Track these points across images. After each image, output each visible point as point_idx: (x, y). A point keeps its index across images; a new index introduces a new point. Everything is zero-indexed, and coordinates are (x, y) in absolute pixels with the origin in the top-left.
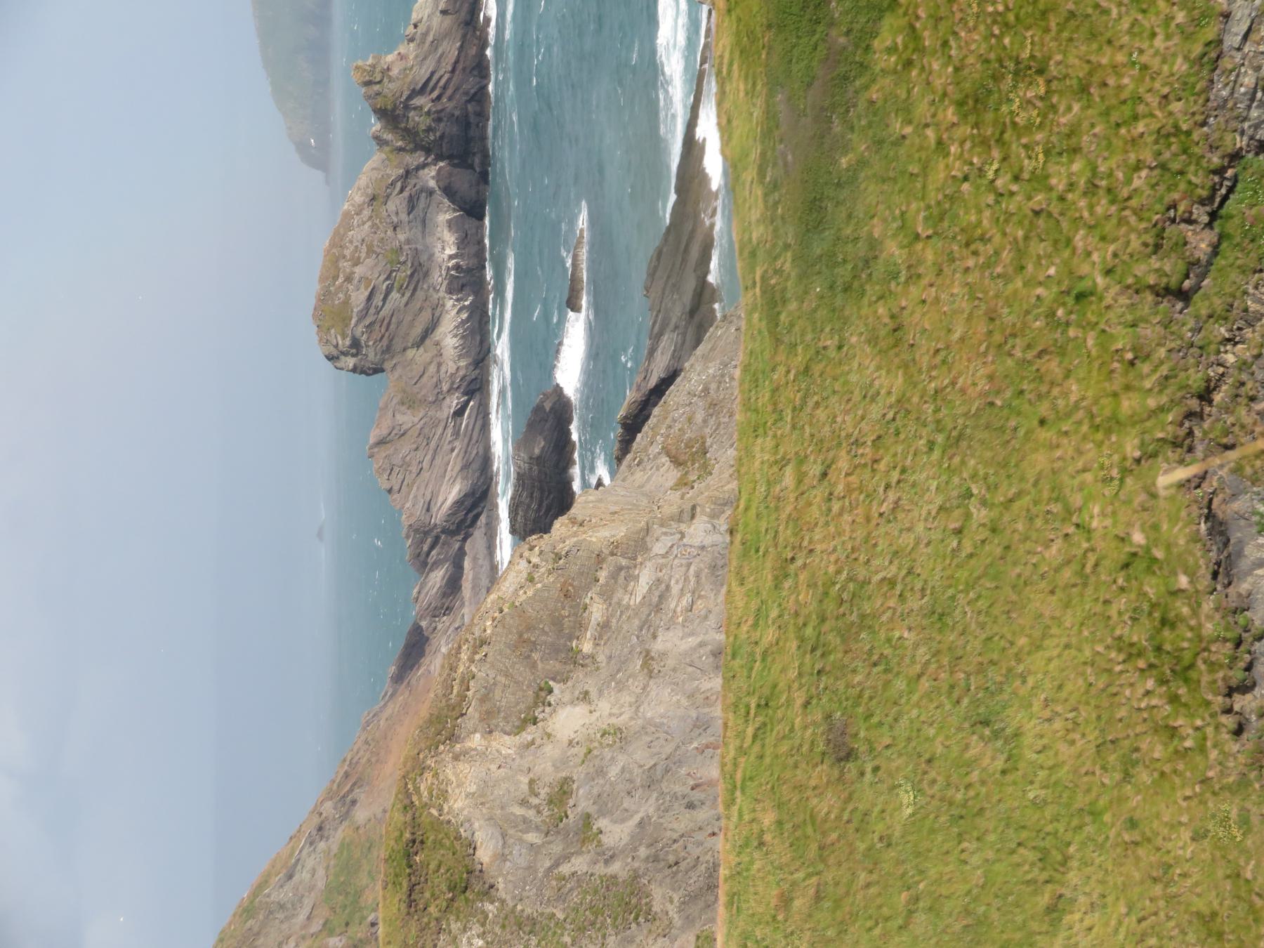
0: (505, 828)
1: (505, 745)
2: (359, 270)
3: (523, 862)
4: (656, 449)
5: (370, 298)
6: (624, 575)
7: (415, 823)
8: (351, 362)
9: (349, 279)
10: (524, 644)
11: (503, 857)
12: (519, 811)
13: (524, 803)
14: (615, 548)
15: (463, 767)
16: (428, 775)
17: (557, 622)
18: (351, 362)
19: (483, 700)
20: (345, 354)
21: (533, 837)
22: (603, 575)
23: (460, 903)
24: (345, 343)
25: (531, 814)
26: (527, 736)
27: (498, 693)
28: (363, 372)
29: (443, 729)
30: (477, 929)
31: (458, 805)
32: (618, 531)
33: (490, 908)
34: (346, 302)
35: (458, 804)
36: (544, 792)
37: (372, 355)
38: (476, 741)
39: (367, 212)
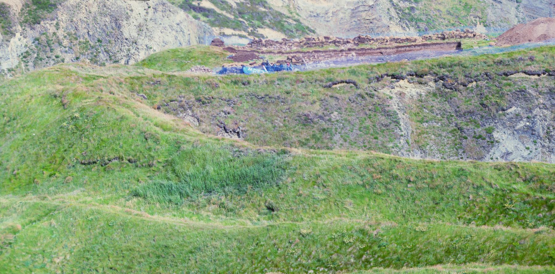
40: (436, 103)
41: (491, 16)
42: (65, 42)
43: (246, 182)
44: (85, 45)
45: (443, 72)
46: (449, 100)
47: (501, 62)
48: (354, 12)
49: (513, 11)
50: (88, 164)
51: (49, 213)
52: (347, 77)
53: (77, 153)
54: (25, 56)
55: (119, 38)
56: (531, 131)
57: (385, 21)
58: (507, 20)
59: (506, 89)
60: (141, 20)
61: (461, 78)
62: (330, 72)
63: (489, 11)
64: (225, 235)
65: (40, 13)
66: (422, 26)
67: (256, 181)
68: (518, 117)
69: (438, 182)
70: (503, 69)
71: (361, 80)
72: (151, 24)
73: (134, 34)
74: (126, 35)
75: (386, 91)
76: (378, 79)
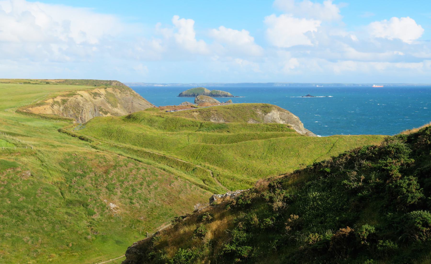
1: (278, 116)
6: (297, 128)
8: (196, 99)
10: (289, 118)
14: (299, 127)
17: (291, 121)
18: (196, 99)
24: (198, 99)
29: (279, 110)
32: (301, 127)
35: (273, 111)
37: (197, 102)
38: (278, 113)
40: (200, 115)
41: (119, 102)
43: (220, 128)
48: (101, 102)
50: (183, 126)
51: (189, 134)
54: (63, 110)
55: (79, 107)
56: (215, 119)
67: (223, 127)
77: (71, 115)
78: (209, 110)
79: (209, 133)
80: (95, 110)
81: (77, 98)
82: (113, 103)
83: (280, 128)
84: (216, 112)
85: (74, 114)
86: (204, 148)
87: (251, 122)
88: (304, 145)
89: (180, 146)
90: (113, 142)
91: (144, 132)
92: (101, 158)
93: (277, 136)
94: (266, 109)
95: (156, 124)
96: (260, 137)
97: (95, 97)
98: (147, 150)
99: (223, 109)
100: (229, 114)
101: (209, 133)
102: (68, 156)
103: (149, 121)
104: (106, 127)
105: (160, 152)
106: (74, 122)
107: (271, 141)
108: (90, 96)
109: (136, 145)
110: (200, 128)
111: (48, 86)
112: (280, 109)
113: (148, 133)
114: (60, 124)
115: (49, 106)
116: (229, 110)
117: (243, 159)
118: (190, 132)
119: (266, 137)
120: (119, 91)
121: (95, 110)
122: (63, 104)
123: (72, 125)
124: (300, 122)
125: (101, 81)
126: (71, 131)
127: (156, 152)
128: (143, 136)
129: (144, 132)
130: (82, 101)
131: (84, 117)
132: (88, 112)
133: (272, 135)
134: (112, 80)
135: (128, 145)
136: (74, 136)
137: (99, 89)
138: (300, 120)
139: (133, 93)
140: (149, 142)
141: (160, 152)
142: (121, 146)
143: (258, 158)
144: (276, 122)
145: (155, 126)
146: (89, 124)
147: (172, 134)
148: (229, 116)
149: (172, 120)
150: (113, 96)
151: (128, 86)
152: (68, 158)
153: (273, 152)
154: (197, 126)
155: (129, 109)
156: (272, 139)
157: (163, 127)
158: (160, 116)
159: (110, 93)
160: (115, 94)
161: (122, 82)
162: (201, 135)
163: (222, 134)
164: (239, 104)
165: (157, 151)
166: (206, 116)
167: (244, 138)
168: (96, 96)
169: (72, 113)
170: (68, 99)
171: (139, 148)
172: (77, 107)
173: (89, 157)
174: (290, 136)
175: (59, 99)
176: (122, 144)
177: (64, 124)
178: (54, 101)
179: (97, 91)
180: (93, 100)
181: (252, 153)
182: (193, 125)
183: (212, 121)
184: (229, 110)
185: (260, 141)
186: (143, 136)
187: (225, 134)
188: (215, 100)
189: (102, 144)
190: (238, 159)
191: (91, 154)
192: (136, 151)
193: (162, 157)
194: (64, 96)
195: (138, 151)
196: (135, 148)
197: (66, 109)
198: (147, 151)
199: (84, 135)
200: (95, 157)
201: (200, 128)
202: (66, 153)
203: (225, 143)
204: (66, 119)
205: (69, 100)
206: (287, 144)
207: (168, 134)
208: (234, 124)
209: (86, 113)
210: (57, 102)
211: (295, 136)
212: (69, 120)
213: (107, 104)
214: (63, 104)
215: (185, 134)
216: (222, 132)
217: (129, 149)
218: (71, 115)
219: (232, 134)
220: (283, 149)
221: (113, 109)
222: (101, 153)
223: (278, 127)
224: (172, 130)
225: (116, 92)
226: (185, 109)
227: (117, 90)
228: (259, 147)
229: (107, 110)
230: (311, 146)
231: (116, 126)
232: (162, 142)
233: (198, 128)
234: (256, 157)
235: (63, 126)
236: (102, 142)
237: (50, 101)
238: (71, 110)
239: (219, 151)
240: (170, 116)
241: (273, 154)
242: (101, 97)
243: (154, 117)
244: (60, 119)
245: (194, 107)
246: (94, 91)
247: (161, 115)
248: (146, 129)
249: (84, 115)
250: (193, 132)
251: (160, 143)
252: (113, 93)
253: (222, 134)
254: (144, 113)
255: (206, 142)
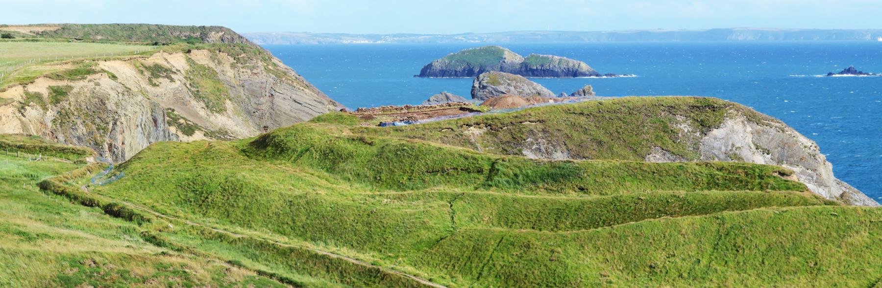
0: (726, 139)
1: (749, 139)
2: (512, 88)
3: (715, 145)
4: (844, 189)
5: (503, 93)
7: (720, 108)
8: (477, 85)
9: (509, 84)
10: (783, 145)
11: (715, 138)
12: (730, 143)
13: (733, 145)
14: (820, 175)
15: (741, 125)
16: (736, 112)
17: (792, 156)
18: (477, 85)
19: (763, 131)
20: (480, 83)
21: (723, 149)
22: (809, 171)
23: (697, 124)
24: (484, 83)
25: (730, 148)
26: (753, 146)
27: (766, 136)
28: (472, 90)
29: (751, 118)
30: (690, 130)
31: (729, 122)
32: (824, 176)
33: (698, 134)
34: (500, 84)
35: (729, 123)
36: (737, 152)
37: (480, 93)
38: (749, 129)
39: (534, 91)
40: (488, 137)
41: (232, 95)
42: (76, 113)
43: (557, 177)
44: (87, 115)
45: (489, 122)
46: (496, 136)
47: (516, 117)
49: (242, 92)
50: (434, 172)
51: (456, 197)
52: (448, 126)
53: (420, 166)
54: (54, 121)
55: (106, 110)
56: (540, 150)
57: (188, 98)
58: (240, 97)
59: (524, 130)
60: (116, 100)
61: (500, 125)
62: (438, 123)
63: (229, 91)
64: (591, 202)
65: (59, 97)
66: (206, 100)
67: (563, 176)
68: (532, 143)
69: (672, 172)
70: (519, 120)
71: (454, 127)
72: (123, 103)
73: (114, 108)
74: (109, 108)
75: (466, 132)
76: (462, 126)
77: (79, 138)
78: (517, 121)
79: (519, 195)
80: (155, 121)
81: (98, 84)
82: (212, 97)
83: (754, 177)
84: (540, 126)
85: (91, 133)
86: (503, 243)
87: (656, 158)
88: (834, 234)
89: (425, 235)
90: (213, 223)
91: (309, 189)
92: (175, 272)
93: (743, 204)
94: (706, 115)
95: (349, 166)
96: (687, 208)
97: (155, 81)
98: (319, 249)
99: (564, 115)
100: (585, 131)
101: (519, 195)
102: (72, 266)
103: (325, 155)
104: (188, 175)
105: (361, 256)
106: (90, 160)
107: (723, 219)
108: (139, 77)
109: (283, 233)
110: (489, 178)
111: (9, 43)
112: (755, 116)
113: (322, 192)
114: (47, 167)
115: (10, 110)
116: (582, 120)
117: (630, 278)
118: (458, 190)
119: (704, 209)
120: (232, 60)
121: (155, 121)
122: (56, 102)
123: (83, 168)
124: (822, 157)
125: (174, 28)
126: (81, 188)
127: (347, 254)
128: (307, 203)
129: (309, 189)
130: (113, 94)
131: (119, 144)
132: (133, 127)
133: (728, 202)
134: (208, 25)
135: (258, 234)
136: (89, 203)
137: (166, 55)
138: (822, 151)
139: (275, 65)
140: (326, 224)
141: (361, 256)
142: (237, 236)
143: (681, 276)
144: (739, 159)
145: (344, 170)
146: (137, 166)
147: (399, 198)
148: (584, 137)
149: (399, 152)
150: (211, 74)
151: (258, 42)
152: (70, 272)
153: (730, 256)
154: (480, 171)
155: (261, 118)
156: (726, 213)
157: (370, 174)
158: (362, 140)
159: (203, 68)
160: (218, 69)
161: (238, 30)
162: (494, 200)
163: (562, 198)
164: (616, 99)
165: (353, 253)
166: (508, 137)
167: (635, 211)
168: (158, 77)
169: (82, 130)
170: (71, 88)
171: (296, 243)
172: (100, 114)
173: (138, 270)
174: (789, 203)
175: (41, 87)
176: (239, 229)
177: (56, 166)
178: (27, 93)
179: (160, 62)
180: (149, 88)
181: (659, 258)
182: (470, 169)
183: (529, 155)
184: (583, 118)
185: (685, 221)
186: (307, 203)
187: (572, 196)
188: (539, 87)
189: (178, 228)
190: (613, 278)
191: (144, 260)
192: (285, 253)
193: (370, 271)
194: (58, 77)
195: (292, 250)
196: (283, 241)
197: (63, 118)
198: (320, 253)
199: (119, 202)
200: (152, 271)
201: (489, 178)
202: (64, 258)
203: (572, 226)
204: (63, 150)
205: (75, 90)
206: (776, 232)
207: (387, 197)
208: (598, 163)
209: (127, 133)
210: (38, 97)
211: (806, 203)
212: (74, 152)
213: (194, 102)
214: (56, 102)
215: (441, 196)
216: (561, 191)
217: (262, 246)
218: (79, 139)
219: (594, 197)
220: (763, 248)
221: (212, 118)
222: (174, 259)
223: (747, 174)
224: (401, 186)
225: (219, 63)
226: (439, 115)
227: (223, 56)
228: (682, 240)
229: (192, 120)
230: (858, 237)
231: (220, 172)
232: (368, 224)
233: (482, 177)
234: (674, 273)
235: (56, 173)
236: (177, 224)
237: (16, 93)
238: (79, 122)
239: (552, 251)
240: (394, 140)
241: (731, 264)
242: (172, 80)
243: (342, 144)
244: (44, 150)
245: (471, 111)
246: (150, 61)
247: (365, 136)
248: (315, 180)
249: (120, 137)
250: (469, 190)
251: (359, 227)
252: (212, 65)
253: (562, 198)
254: (311, 130)
255: (510, 224)
